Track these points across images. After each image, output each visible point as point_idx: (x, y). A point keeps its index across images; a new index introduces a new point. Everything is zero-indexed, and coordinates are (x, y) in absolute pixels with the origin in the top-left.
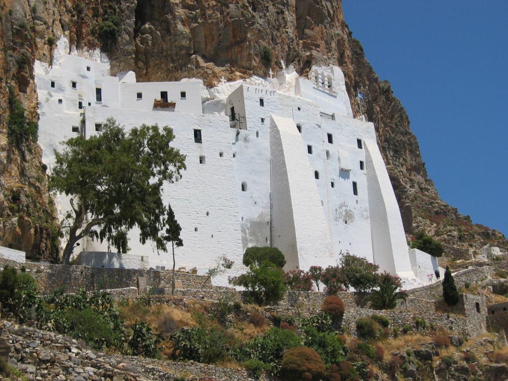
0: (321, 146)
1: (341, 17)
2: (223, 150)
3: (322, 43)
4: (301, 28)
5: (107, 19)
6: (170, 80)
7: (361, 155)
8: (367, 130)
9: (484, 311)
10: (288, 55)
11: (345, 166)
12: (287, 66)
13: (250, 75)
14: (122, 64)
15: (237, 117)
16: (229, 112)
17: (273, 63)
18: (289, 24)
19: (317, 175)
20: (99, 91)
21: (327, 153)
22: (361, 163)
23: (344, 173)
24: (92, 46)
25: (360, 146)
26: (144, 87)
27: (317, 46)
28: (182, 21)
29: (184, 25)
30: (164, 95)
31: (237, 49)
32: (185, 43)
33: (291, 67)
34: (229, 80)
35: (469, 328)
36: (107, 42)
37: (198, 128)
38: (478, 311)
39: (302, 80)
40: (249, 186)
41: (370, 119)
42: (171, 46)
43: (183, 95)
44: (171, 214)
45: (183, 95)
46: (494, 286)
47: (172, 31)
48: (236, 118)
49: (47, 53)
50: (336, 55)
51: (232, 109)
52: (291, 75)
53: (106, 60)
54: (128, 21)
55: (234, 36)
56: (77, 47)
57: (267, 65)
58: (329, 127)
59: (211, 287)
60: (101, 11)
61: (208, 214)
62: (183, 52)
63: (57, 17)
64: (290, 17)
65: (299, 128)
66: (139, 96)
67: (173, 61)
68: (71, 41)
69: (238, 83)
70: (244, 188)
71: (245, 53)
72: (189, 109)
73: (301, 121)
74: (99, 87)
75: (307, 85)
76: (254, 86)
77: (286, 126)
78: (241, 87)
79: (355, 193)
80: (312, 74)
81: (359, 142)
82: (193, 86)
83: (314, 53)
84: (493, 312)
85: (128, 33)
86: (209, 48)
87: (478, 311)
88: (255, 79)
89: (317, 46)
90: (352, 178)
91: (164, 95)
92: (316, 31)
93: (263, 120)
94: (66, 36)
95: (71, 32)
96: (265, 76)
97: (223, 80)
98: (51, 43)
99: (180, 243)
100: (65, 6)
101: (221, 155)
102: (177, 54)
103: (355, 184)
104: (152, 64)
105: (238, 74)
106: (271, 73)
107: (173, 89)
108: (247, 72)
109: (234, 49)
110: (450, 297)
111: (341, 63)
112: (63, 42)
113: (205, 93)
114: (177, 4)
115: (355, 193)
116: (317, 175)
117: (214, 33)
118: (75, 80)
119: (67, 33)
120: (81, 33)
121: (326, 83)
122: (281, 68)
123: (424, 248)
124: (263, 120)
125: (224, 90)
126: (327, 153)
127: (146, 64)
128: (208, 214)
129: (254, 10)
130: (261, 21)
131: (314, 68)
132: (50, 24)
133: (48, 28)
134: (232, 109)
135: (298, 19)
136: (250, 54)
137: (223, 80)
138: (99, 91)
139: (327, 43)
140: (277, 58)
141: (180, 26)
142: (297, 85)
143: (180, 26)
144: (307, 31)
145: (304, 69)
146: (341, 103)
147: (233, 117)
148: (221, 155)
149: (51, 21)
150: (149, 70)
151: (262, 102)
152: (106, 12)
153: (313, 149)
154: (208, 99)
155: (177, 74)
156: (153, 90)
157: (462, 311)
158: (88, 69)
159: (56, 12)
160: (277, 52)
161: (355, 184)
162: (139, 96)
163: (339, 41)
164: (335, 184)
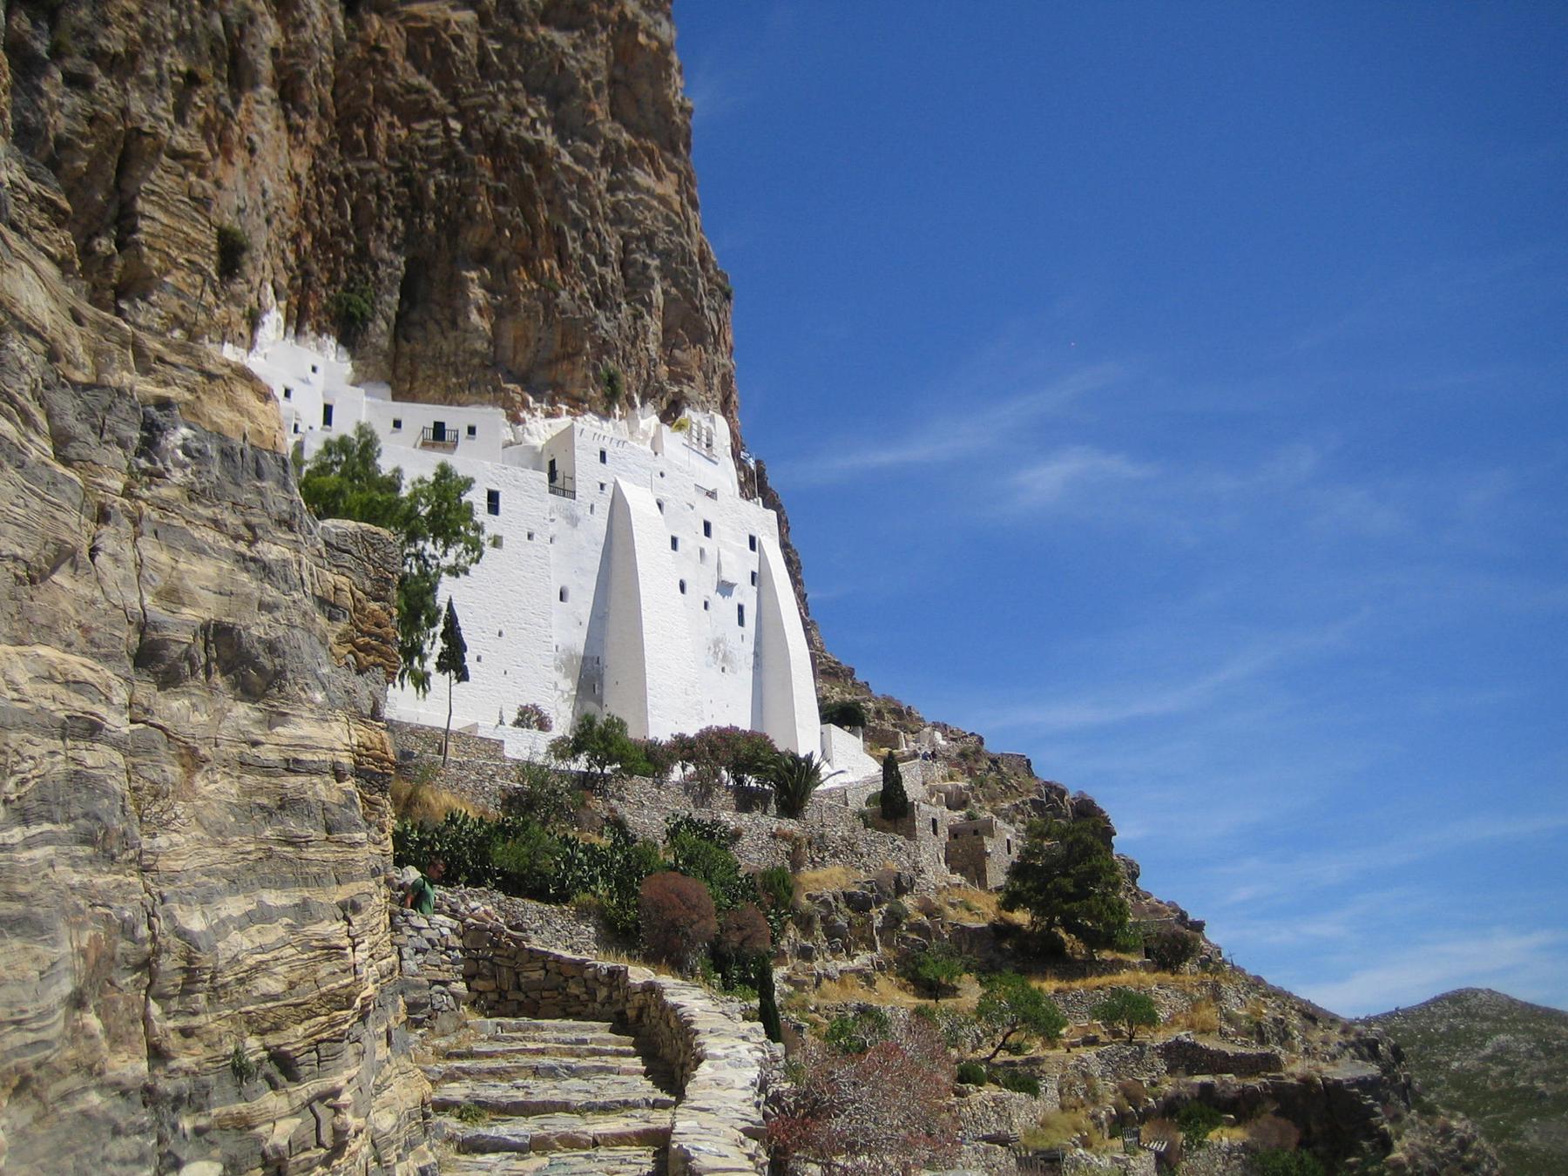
0: (692, 540)
1: (729, 338)
2: (534, 528)
3: (699, 376)
4: (669, 342)
5: (352, 291)
6: (450, 404)
8: (763, 521)
9: (944, 834)
10: (647, 385)
11: (727, 576)
12: (642, 404)
13: (584, 412)
14: (371, 369)
15: (559, 475)
16: (547, 467)
17: (622, 398)
18: (651, 337)
19: (682, 587)
20: (328, 410)
21: (702, 551)
22: (753, 574)
23: (725, 588)
24: (320, 330)
25: (753, 547)
26: (405, 410)
27: (691, 379)
28: (480, 310)
29: (482, 316)
31: (565, 366)
32: (481, 346)
33: (649, 406)
34: (549, 415)
35: (924, 859)
36: (348, 329)
37: (494, 487)
38: (935, 832)
39: (665, 428)
40: (571, 594)
42: (457, 347)
43: (472, 430)
44: (452, 621)
45: (472, 430)
46: (947, 795)
47: (461, 323)
48: (558, 480)
49: (245, 332)
50: (719, 397)
51: (552, 463)
52: (649, 420)
53: (346, 357)
54: (387, 297)
55: (564, 345)
56: (299, 332)
57: (611, 397)
58: (706, 510)
59: (504, 759)
60: (344, 275)
61: (500, 634)
62: (476, 361)
63: (268, 274)
64: (655, 325)
65: (660, 505)
66: (397, 424)
67: (457, 374)
68: (288, 320)
69: (564, 421)
70: (562, 596)
71: (579, 375)
72: (493, 449)
73: (664, 495)
74: (329, 402)
75: (673, 440)
76: (590, 429)
77: (639, 500)
78: (570, 431)
81: (752, 540)
83: (686, 389)
84: (956, 836)
85: (387, 319)
86: (519, 358)
87: (935, 832)
88: (590, 417)
89: (691, 379)
90: (736, 599)
91: (439, 429)
92: (688, 355)
93: (602, 486)
94: (279, 308)
95: (289, 304)
96: (606, 415)
97: (539, 414)
98: (254, 320)
99: (463, 676)
100: (284, 259)
101: (530, 536)
102: (464, 364)
103: (741, 608)
104: (420, 375)
105: (565, 407)
106: (617, 411)
107: (455, 417)
108: (578, 404)
109: (557, 367)
110: (891, 807)
111: (725, 409)
112: (273, 320)
113: (507, 433)
114: (472, 280)
116: (682, 587)
117: (530, 334)
118: (289, 386)
119: (283, 304)
120: (307, 307)
121: (704, 439)
122: (633, 406)
123: (840, 723)
124: (602, 486)
125: (540, 429)
126: (702, 551)
127: (413, 376)
128: (500, 634)
129: (598, 305)
130: (607, 326)
131: (688, 412)
132: (257, 284)
133: (251, 291)
134: (552, 463)
135: (665, 331)
136: (586, 377)
137: (539, 414)
138: (328, 410)
139: (706, 377)
140: (629, 388)
141: (475, 317)
143: (475, 317)
144: (677, 352)
145: (671, 414)
146: (725, 476)
147: (553, 476)
148: (530, 536)
149: (258, 280)
150: (416, 384)
151: (603, 455)
152: (351, 279)
153: (679, 543)
154: (511, 444)
155: (465, 396)
156: (420, 416)
157: (911, 834)
158: (314, 369)
159: (268, 267)
160: (628, 378)
161: (741, 608)
162: (397, 424)
163: (724, 376)
164: (710, 605)
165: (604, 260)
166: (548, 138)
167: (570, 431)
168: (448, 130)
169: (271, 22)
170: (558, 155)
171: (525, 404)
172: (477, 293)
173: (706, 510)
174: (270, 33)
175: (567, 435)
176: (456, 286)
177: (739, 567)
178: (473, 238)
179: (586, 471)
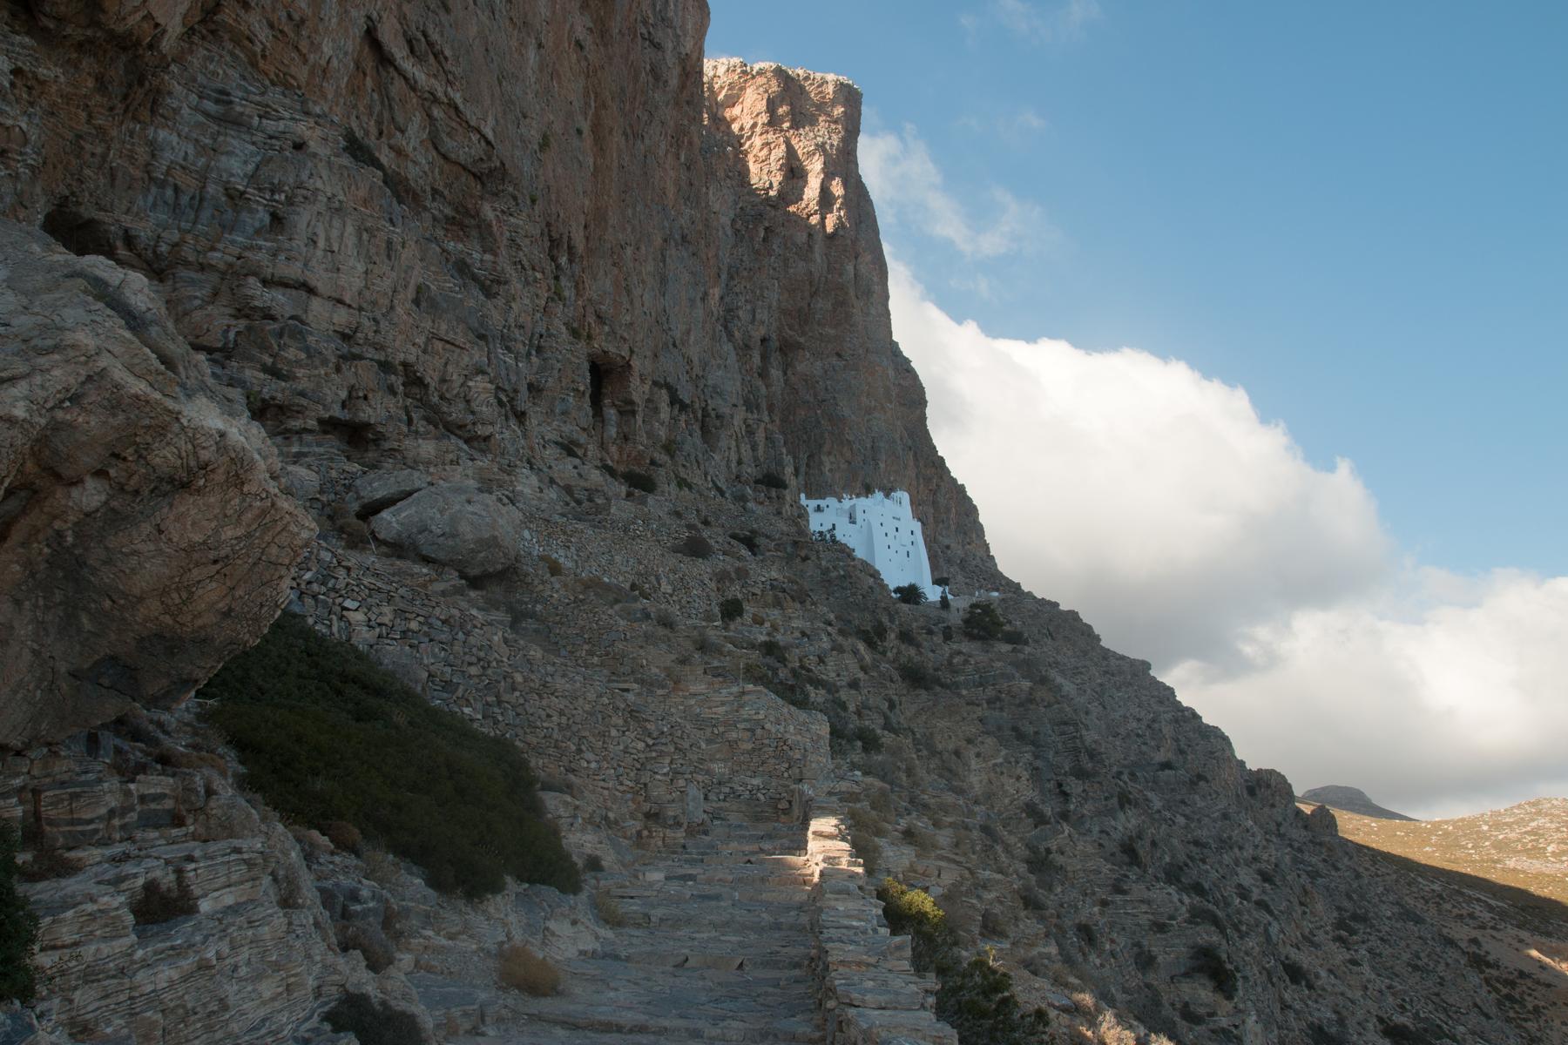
0: (892, 533)
8: (917, 526)
48: (853, 521)
57: (868, 491)
82: (831, 501)
107: (822, 503)
108: (858, 496)
110: (944, 603)
113: (838, 505)
125: (847, 503)
166: (847, 412)
172: (828, 466)
173: (897, 523)
174: (763, 390)
176: (821, 463)
177: (907, 539)
178: (826, 448)
179: (859, 516)
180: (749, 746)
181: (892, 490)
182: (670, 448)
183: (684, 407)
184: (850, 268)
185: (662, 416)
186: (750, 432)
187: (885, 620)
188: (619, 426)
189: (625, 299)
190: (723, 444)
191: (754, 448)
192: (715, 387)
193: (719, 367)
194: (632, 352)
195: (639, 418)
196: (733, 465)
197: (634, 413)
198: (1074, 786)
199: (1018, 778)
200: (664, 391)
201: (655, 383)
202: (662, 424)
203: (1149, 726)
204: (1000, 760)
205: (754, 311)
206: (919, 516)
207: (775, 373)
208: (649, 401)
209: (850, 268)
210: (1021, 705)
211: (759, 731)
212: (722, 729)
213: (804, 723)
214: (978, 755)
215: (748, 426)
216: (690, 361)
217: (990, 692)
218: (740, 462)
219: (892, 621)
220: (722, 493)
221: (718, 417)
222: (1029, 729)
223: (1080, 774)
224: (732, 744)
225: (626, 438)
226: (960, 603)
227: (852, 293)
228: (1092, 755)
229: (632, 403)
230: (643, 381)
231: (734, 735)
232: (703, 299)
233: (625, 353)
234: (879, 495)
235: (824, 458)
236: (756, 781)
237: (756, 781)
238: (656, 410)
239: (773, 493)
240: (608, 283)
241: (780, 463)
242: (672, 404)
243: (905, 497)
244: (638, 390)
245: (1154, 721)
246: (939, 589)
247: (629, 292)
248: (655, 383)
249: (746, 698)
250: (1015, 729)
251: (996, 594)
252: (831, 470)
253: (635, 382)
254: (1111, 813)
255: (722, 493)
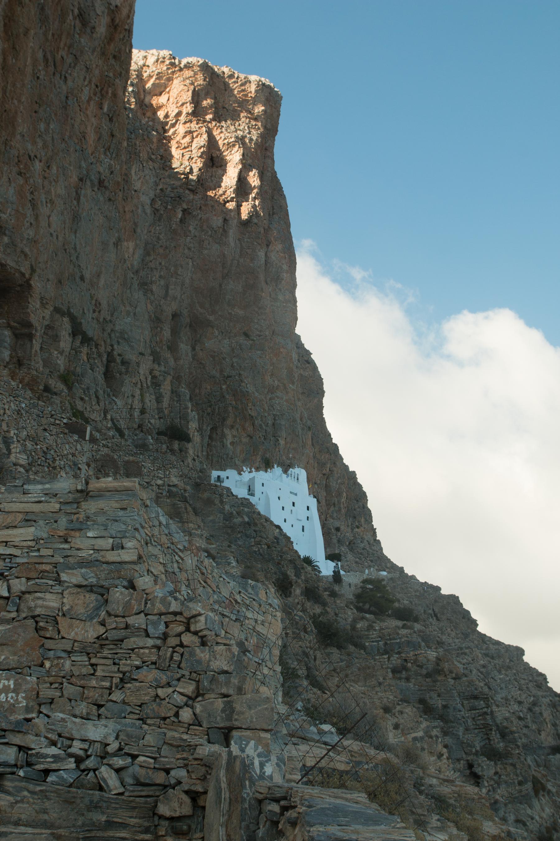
0: (288, 507)
7: (308, 513)
8: (313, 503)
30: (219, 477)
34: (249, 472)
39: (284, 476)
41: (315, 497)
45: (228, 478)
57: (267, 465)
69: (254, 474)
78: (254, 477)
79: (303, 530)
80: (289, 472)
82: (231, 473)
91: (219, 477)
96: (266, 471)
103: (303, 527)
108: (257, 469)
113: (238, 477)
115: (303, 530)
125: (246, 476)
142: (281, 476)
146: (303, 486)
147: (249, 490)
151: (263, 484)
161: (303, 527)
165: (267, 426)
166: (251, 389)
167: (254, 477)
168: (221, 389)
169: (172, 360)
170: (254, 393)
171: (243, 470)
173: (293, 498)
175: (252, 480)
176: (223, 436)
178: (229, 422)
180: (90, 632)
181: (291, 466)
182: (67, 379)
183: (86, 340)
184: (261, 254)
185: (62, 344)
186: (156, 384)
187: (291, 573)
188: (13, 349)
189: (29, 213)
190: (127, 389)
191: (159, 400)
192: (122, 332)
193: (128, 313)
194: (33, 270)
195: (36, 344)
196: (136, 414)
197: (30, 337)
198: (486, 768)
199: (440, 756)
200: (66, 319)
201: (57, 310)
202: (61, 353)
203: (530, 710)
204: (420, 734)
205: (167, 287)
206: (313, 492)
207: (184, 347)
208: (48, 327)
209: (261, 254)
210: (428, 675)
211: (119, 594)
212: (19, 585)
213: (232, 603)
214: (396, 727)
215: (154, 377)
216: (98, 304)
217: (395, 660)
218: (143, 411)
219: (298, 575)
220: (122, 435)
221: (123, 363)
222: (438, 703)
223: (493, 755)
224: (43, 626)
225: (20, 363)
226: (352, 579)
227: (262, 277)
228: (504, 734)
229: (30, 325)
230: (43, 305)
231: (50, 602)
232: (116, 245)
233: (25, 268)
234: (278, 470)
235: (227, 431)
236: (96, 731)
237: (96, 731)
238: (56, 338)
239: (176, 445)
240: (11, 191)
241: (184, 417)
242: (74, 334)
243: (302, 474)
244: (38, 315)
245: (534, 704)
246: (331, 565)
247: (34, 206)
248: (57, 310)
249: (90, 507)
250: (422, 701)
251: (385, 573)
252: (232, 443)
253: (34, 303)
254: (525, 799)
255: (122, 435)
